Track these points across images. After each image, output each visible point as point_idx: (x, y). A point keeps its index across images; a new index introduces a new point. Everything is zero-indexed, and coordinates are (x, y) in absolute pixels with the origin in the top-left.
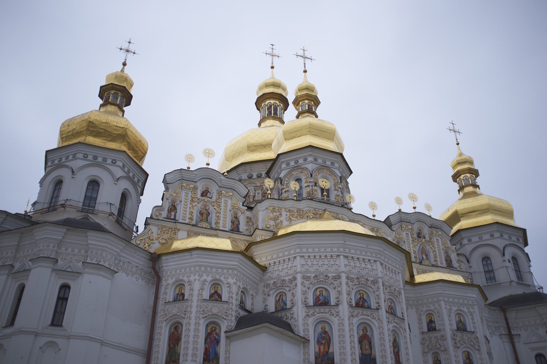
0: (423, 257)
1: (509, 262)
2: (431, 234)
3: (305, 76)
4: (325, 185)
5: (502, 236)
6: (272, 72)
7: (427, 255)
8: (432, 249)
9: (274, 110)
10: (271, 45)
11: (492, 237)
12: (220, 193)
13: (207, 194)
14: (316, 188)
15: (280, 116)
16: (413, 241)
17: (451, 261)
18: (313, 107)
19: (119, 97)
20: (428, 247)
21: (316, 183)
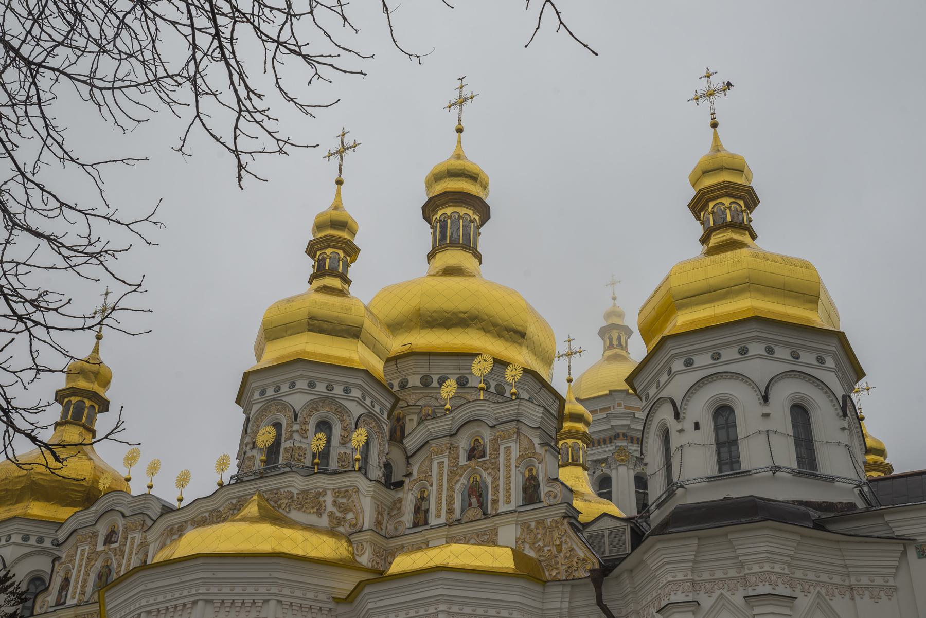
0: (470, 504)
1: (697, 426)
2: (495, 440)
3: (338, 193)
4: (265, 440)
5: (689, 363)
6: (459, 142)
7: (481, 495)
8: (492, 475)
9: (440, 232)
10: (463, 78)
11: (742, 354)
12: (126, 529)
13: (111, 538)
14: (255, 452)
15: (455, 236)
16: (452, 475)
17: (537, 487)
18: (328, 260)
19: (72, 406)
20: (484, 474)
21: (254, 443)
